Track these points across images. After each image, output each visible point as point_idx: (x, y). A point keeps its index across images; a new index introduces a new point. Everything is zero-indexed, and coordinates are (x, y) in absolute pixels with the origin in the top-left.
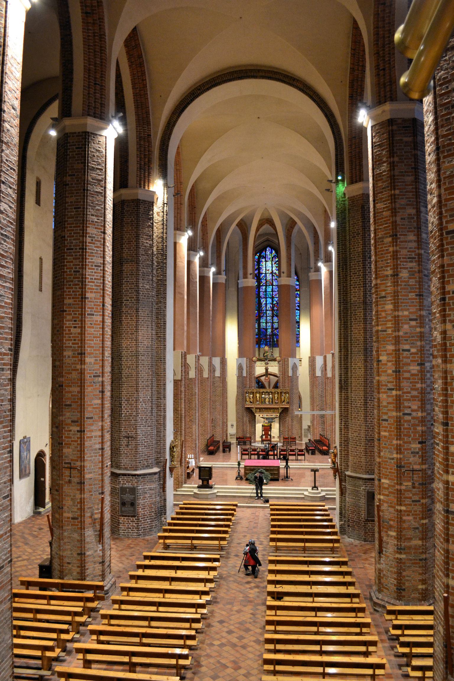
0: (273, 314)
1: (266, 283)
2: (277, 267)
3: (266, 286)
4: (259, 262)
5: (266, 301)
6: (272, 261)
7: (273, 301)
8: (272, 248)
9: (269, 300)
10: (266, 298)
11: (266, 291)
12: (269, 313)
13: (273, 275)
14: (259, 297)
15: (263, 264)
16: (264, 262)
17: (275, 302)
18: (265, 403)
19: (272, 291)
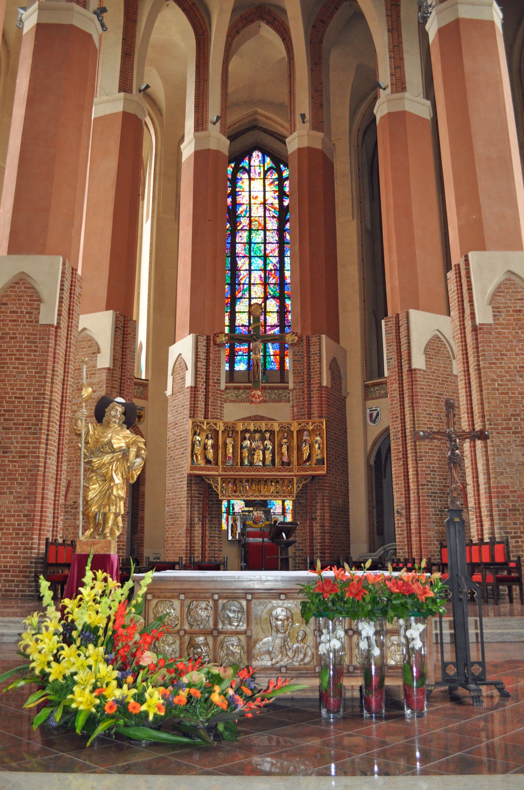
0: (265, 292)
1: (250, 224)
2: (275, 192)
3: (250, 230)
4: (234, 181)
5: (250, 264)
6: (264, 179)
7: (265, 264)
8: (265, 153)
9: (258, 263)
10: (250, 257)
11: (250, 243)
12: (258, 291)
13: (265, 209)
14: (234, 256)
15: (243, 184)
16: (247, 182)
17: (270, 267)
18: (251, 463)
19: (265, 243)
